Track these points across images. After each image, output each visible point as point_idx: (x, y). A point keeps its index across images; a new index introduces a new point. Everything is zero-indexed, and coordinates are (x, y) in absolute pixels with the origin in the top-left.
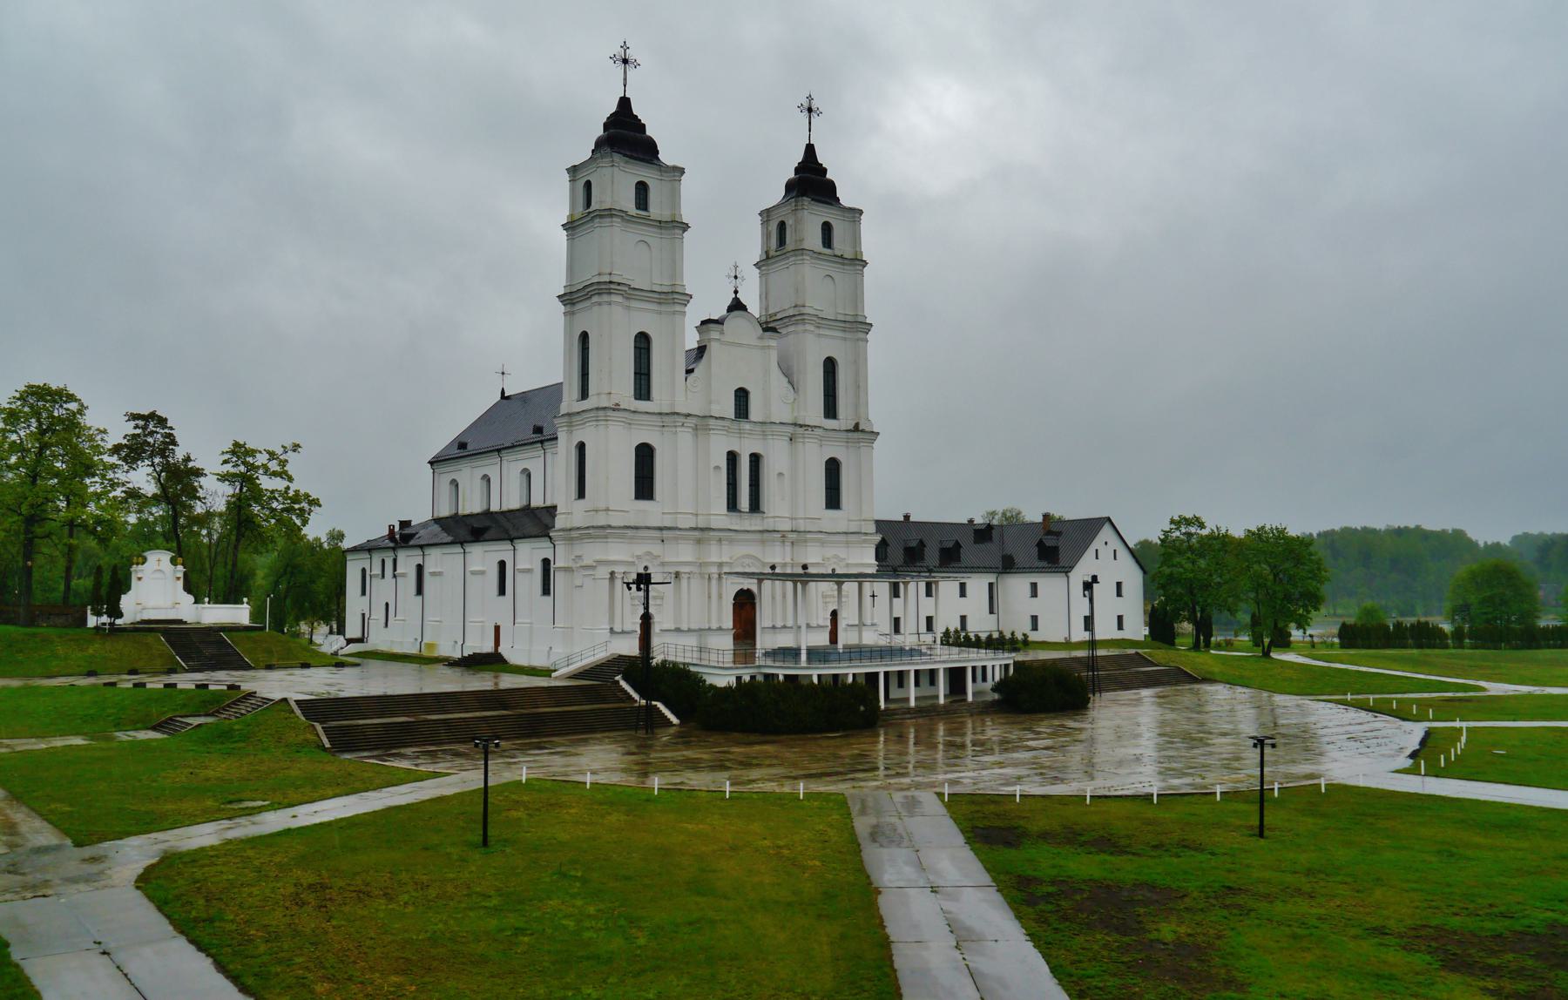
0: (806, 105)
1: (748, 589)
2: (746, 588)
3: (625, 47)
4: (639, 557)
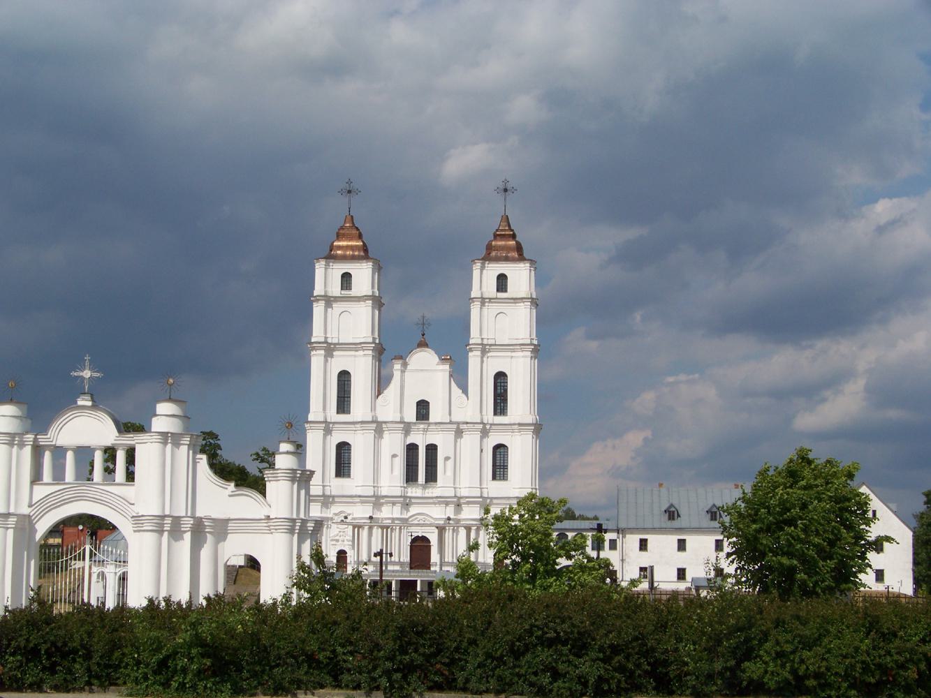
0: (502, 187)
1: (423, 536)
2: (420, 535)
3: (349, 182)
4: (336, 514)
